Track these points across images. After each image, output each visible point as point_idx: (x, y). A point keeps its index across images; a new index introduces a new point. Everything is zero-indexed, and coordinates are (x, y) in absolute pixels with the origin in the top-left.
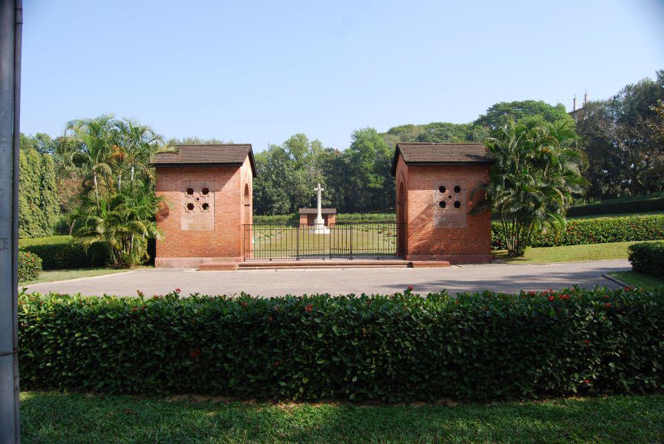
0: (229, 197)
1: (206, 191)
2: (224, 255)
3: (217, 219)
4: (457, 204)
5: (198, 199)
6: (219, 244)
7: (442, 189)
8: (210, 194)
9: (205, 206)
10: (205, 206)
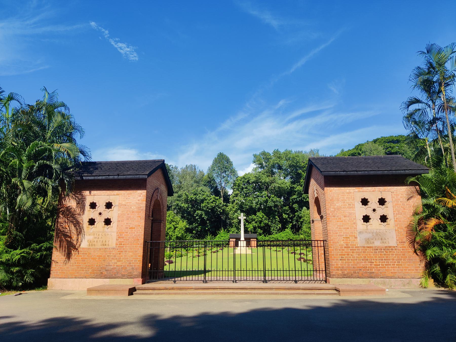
0: (133, 212)
1: (109, 205)
2: (123, 277)
4: (384, 219)
5: (100, 214)
6: (119, 263)
7: (365, 202)
8: (114, 208)
10: (108, 222)
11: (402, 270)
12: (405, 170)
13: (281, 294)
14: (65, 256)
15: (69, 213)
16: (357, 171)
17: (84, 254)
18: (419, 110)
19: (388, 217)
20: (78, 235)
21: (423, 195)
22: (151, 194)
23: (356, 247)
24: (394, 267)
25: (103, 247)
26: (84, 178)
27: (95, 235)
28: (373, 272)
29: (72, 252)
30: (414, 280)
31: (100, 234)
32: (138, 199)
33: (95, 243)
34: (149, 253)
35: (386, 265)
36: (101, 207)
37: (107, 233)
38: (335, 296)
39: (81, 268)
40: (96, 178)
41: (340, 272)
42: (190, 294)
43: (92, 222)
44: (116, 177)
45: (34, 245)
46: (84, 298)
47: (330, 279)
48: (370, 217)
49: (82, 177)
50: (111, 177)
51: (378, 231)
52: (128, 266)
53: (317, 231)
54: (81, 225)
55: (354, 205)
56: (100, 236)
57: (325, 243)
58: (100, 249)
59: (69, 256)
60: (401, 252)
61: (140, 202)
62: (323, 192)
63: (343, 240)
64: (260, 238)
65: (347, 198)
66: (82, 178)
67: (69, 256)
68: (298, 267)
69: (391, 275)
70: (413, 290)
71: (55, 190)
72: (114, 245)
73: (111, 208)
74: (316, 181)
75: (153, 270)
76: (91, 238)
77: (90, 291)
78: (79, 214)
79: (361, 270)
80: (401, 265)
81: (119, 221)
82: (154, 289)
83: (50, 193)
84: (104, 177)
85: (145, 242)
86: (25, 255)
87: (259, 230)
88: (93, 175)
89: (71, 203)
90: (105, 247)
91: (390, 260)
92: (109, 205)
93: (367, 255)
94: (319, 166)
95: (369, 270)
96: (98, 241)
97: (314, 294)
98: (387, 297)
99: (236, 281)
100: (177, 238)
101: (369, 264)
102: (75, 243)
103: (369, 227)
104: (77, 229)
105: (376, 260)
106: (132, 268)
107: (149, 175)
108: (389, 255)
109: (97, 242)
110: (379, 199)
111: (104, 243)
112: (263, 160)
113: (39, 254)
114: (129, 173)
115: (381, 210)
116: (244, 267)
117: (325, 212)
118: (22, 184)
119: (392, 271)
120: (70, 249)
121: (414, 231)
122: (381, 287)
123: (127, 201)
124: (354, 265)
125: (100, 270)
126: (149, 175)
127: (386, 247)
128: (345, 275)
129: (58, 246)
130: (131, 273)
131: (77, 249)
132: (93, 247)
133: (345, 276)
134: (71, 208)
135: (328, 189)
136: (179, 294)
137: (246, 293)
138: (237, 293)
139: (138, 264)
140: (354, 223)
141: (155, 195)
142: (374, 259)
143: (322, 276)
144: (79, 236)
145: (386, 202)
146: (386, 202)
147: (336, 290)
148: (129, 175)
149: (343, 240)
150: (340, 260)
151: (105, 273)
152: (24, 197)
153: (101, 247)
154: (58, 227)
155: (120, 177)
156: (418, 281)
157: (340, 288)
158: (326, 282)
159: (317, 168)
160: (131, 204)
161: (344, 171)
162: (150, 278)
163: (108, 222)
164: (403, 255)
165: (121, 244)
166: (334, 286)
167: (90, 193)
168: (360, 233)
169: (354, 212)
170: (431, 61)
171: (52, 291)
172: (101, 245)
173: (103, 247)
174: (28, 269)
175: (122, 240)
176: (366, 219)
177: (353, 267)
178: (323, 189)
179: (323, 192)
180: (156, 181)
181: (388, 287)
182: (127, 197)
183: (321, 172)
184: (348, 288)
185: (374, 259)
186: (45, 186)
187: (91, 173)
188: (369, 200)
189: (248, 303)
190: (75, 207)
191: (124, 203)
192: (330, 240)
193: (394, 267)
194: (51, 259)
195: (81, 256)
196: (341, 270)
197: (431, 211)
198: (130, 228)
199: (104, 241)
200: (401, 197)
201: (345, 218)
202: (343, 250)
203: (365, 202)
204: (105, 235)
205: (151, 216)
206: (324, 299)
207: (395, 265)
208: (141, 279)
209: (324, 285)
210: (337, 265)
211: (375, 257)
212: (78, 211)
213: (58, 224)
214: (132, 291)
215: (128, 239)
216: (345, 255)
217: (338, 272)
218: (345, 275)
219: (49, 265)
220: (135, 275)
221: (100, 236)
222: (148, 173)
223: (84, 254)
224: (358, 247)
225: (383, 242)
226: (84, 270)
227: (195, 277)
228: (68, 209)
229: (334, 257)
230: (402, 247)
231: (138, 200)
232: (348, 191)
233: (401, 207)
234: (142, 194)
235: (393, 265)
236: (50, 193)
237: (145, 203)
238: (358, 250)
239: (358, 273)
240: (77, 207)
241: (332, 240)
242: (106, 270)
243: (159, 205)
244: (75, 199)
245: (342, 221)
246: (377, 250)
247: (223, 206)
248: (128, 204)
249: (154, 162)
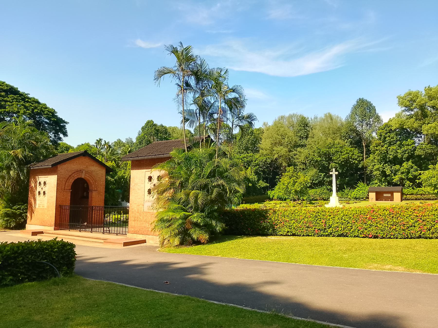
8: (47, 185)
64: (405, 191)
87: (408, 182)
100: (296, 191)
112: (409, 102)
247: (358, 157)
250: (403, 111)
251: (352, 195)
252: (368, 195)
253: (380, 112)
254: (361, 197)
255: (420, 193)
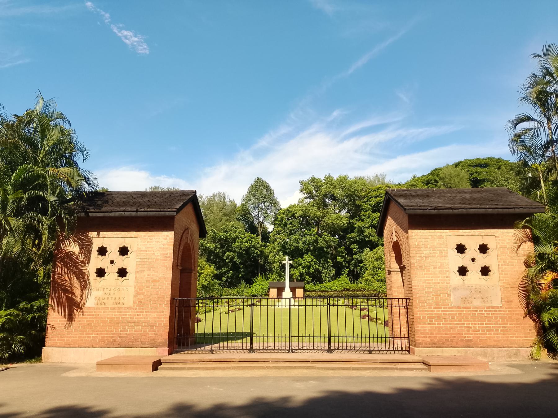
0: (157, 260)
1: (124, 251)
3: (139, 291)
4: (485, 271)
5: (112, 262)
6: (137, 328)
7: (461, 249)
9: (122, 273)
11: (508, 337)
12: (514, 208)
13: (354, 369)
14: (65, 317)
15: (70, 262)
16: (452, 209)
17: (89, 315)
18: (531, 129)
19: (490, 269)
20: (82, 290)
21: (535, 240)
22: (180, 236)
23: (449, 308)
24: (497, 334)
25: (116, 306)
26: (90, 214)
27: (105, 290)
28: (471, 340)
29: (75, 311)
30: (523, 350)
31: (112, 289)
32: (163, 243)
33: (105, 301)
34: (177, 314)
35: (487, 331)
36: (113, 253)
37: (121, 288)
38: (424, 371)
39: (87, 334)
40: (106, 214)
41: (428, 340)
42: (234, 368)
43: (101, 273)
44: (134, 214)
45: (23, 304)
46: (93, 375)
47: (416, 349)
48: (468, 269)
49: (87, 213)
50: (127, 214)
51: (478, 287)
52: (149, 331)
53: (396, 285)
54: (86, 277)
55: (447, 253)
56: (112, 292)
57: (408, 301)
58: (112, 309)
59: (71, 318)
60: (507, 314)
61: (166, 247)
62: (406, 236)
63: (433, 299)
64: (308, 287)
65: (437, 244)
66: (88, 215)
67: (71, 318)
68: (373, 332)
69: (493, 343)
70: (523, 363)
71: (52, 231)
72: (131, 304)
73: (127, 255)
74: (396, 220)
75: (183, 335)
76: (100, 294)
77: (101, 365)
78: (83, 262)
79: (455, 337)
80: (507, 331)
81: (137, 272)
82: (185, 362)
83: (45, 235)
84: (117, 214)
85: (173, 299)
86: (12, 318)
88: (102, 210)
89: (74, 248)
90: (119, 306)
91: (492, 324)
92: (124, 251)
93: (463, 318)
94: (401, 201)
95: (465, 337)
96: (110, 299)
97: (396, 369)
98: (492, 373)
99: (292, 350)
101: (466, 329)
102: (78, 299)
103: (466, 282)
104: (81, 282)
105: (475, 324)
106: (156, 335)
107: (178, 211)
108: (492, 318)
109: (108, 299)
110: (480, 245)
111: (117, 300)
113: (30, 316)
114: (151, 208)
115: (483, 260)
116: (302, 333)
117: (408, 262)
118: (8, 223)
119: (495, 339)
120: (72, 308)
121: (529, 289)
122: (481, 359)
123: (148, 246)
124: (446, 331)
125: (113, 337)
126: (178, 211)
127: (488, 308)
128: (435, 344)
129: (55, 305)
130: (153, 340)
131: (81, 309)
132: (103, 306)
133: (434, 345)
134: (73, 255)
135: (410, 231)
136: (219, 368)
137: (308, 368)
138: (295, 368)
139: (163, 330)
140: (447, 277)
141: (184, 237)
142: (472, 324)
143: (405, 343)
144: (84, 292)
145: (488, 249)
146: (488, 249)
147: (424, 363)
148: (151, 211)
149: (433, 299)
150: (429, 324)
151: (119, 340)
152: (12, 240)
153: (113, 306)
154: (54, 278)
155: (139, 214)
156: (527, 351)
157: (431, 362)
158: (409, 353)
159: (399, 204)
160: (154, 250)
161: (435, 209)
162: (179, 345)
163: (122, 273)
164: (509, 317)
165: (141, 302)
166: (421, 359)
167: (98, 235)
168: (455, 289)
169: (447, 262)
170: (547, 66)
171: (48, 364)
172: (113, 304)
173: (116, 306)
174: (16, 336)
175: (140, 297)
176: (463, 271)
177: (446, 334)
178: (407, 232)
179: (406, 236)
180: (186, 219)
181: (490, 358)
182: (149, 240)
183: (405, 209)
184: (440, 362)
185: (472, 324)
186: (39, 224)
187: (99, 207)
188: (466, 247)
189: (314, 382)
190: (78, 254)
191: (144, 248)
192: (415, 298)
193: (497, 334)
194: (46, 321)
195: (86, 318)
196: (430, 337)
197: (545, 262)
198: (152, 282)
199: (117, 299)
200: (508, 243)
201: (435, 270)
202: (432, 311)
203: (461, 249)
204: (119, 290)
205: (179, 264)
206: (408, 375)
207: (498, 330)
208: (167, 349)
209: (406, 357)
210: (425, 330)
211: (474, 321)
212: (81, 258)
213: (54, 275)
214: (156, 365)
215: (150, 296)
216: (434, 317)
217: (425, 339)
218: (435, 344)
219: (44, 329)
220: (160, 343)
221: (112, 292)
222: (176, 208)
223: (89, 315)
224: (452, 308)
225: (484, 301)
226: (90, 337)
227: (238, 343)
228: (69, 255)
229: (421, 321)
230: (509, 308)
231: (164, 245)
232: (439, 234)
233: (509, 256)
234: (168, 236)
235: (496, 330)
236: (45, 235)
237: (173, 248)
238: (452, 311)
239: (451, 341)
240: (80, 253)
241: (418, 298)
242: (120, 337)
243: (189, 250)
244: (78, 242)
245: (431, 274)
246: (476, 311)
247: (261, 246)
248: (150, 249)
249: (183, 193)
250: (305, 198)
251: (250, 292)
252: (268, 292)
253: (278, 195)
254: (260, 293)
255: (323, 289)
